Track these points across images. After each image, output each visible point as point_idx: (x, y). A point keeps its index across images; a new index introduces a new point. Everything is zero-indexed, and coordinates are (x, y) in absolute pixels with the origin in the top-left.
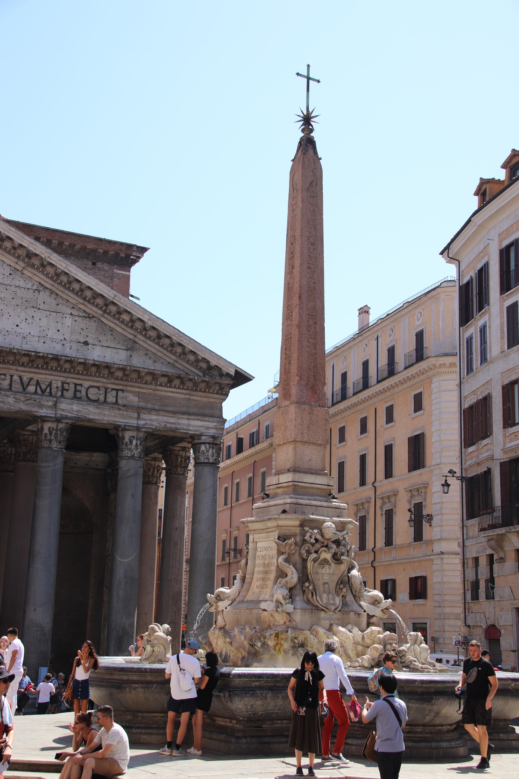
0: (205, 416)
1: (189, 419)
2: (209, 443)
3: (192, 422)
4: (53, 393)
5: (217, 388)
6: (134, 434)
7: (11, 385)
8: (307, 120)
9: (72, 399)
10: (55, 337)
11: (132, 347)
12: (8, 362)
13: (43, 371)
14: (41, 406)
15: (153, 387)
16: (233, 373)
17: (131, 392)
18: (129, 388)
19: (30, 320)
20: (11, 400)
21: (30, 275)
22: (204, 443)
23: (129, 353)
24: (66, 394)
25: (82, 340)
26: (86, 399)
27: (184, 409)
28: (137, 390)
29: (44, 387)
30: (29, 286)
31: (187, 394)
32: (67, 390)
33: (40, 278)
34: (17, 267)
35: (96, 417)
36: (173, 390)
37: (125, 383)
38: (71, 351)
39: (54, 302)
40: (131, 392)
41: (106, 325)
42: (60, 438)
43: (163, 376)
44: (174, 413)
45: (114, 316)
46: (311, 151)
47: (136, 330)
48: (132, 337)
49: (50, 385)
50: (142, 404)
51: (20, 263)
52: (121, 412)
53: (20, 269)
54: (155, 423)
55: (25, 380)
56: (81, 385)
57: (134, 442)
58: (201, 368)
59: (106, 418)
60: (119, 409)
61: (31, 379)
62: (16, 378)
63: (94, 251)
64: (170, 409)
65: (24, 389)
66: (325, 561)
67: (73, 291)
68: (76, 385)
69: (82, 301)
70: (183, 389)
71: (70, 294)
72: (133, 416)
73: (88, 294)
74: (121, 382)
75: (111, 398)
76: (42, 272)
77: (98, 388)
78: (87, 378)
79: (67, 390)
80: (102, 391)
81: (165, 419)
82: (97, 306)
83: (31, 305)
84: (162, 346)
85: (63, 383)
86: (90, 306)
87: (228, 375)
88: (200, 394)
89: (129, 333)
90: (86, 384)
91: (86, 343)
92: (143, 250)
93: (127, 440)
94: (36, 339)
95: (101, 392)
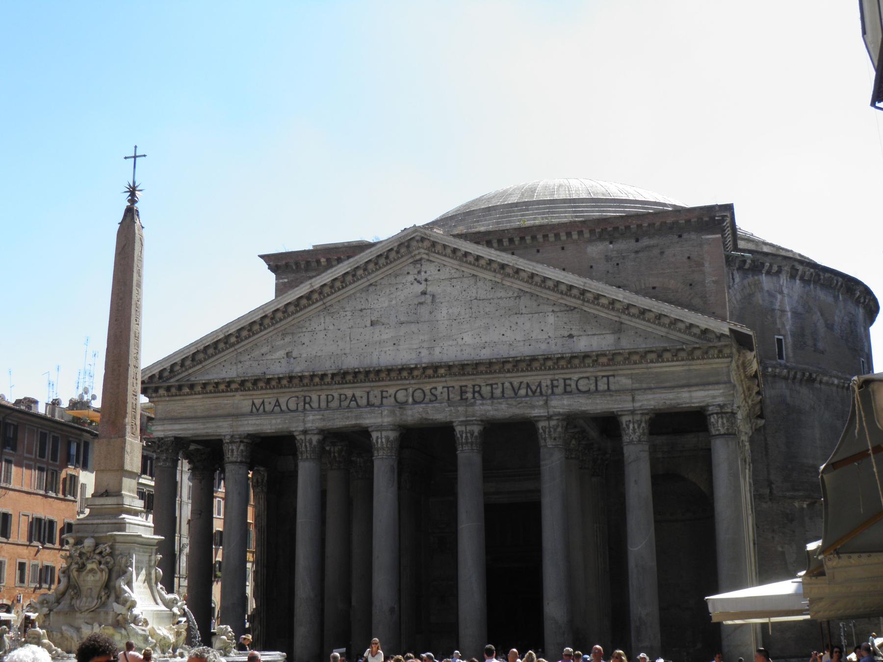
0: (709, 384)
1: (690, 391)
2: (717, 413)
3: (694, 394)
4: (544, 392)
5: (716, 351)
6: (629, 418)
7: (503, 392)
8: (132, 191)
9: (563, 394)
10: (539, 337)
11: (618, 329)
12: (495, 372)
13: (529, 373)
14: (533, 407)
15: (644, 365)
16: (727, 332)
17: (624, 375)
18: (620, 372)
19: (514, 327)
20: (504, 406)
21: (509, 284)
22: (712, 414)
23: (616, 336)
24: (556, 390)
25: (566, 334)
26: (576, 391)
27: (684, 382)
28: (629, 372)
29: (534, 388)
30: (510, 294)
31: (683, 365)
32: (557, 386)
33: (518, 285)
34: (496, 280)
35: (589, 408)
36: (668, 364)
37: (614, 368)
38: (556, 348)
39: (535, 304)
40: (624, 375)
41: (589, 313)
42: (556, 435)
43: (652, 352)
44: (673, 387)
45: (593, 303)
46: (128, 219)
47: (618, 310)
48: (617, 319)
49: (540, 385)
50: (637, 385)
51: (498, 275)
52: (614, 398)
53: (500, 281)
54: (652, 403)
55: (516, 385)
56: (570, 379)
57: (631, 426)
58: (695, 335)
59: (599, 407)
60: (611, 396)
61: (521, 383)
62: (507, 385)
63: (676, 223)
64: (668, 384)
65: (516, 394)
66: (92, 570)
67: (549, 288)
68: (565, 380)
69: (560, 296)
70: (677, 360)
71: (548, 292)
72: (635, 398)
73: (563, 288)
74: (608, 368)
75: (602, 386)
76: (518, 278)
77: (588, 378)
78: (573, 370)
79: (557, 386)
80: (592, 381)
81: (663, 396)
82: (575, 297)
83: (514, 311)
84: (649, 321)
85: (552, 381)
86: (569, 298)
87: (723, 335)
88: (699, 362)
89: (612, 316)
90: (575, 377)
91: (571, 336)
92: (729, 208)
93: (624, 426)
94: (522, 343)
95: (591, 382)
